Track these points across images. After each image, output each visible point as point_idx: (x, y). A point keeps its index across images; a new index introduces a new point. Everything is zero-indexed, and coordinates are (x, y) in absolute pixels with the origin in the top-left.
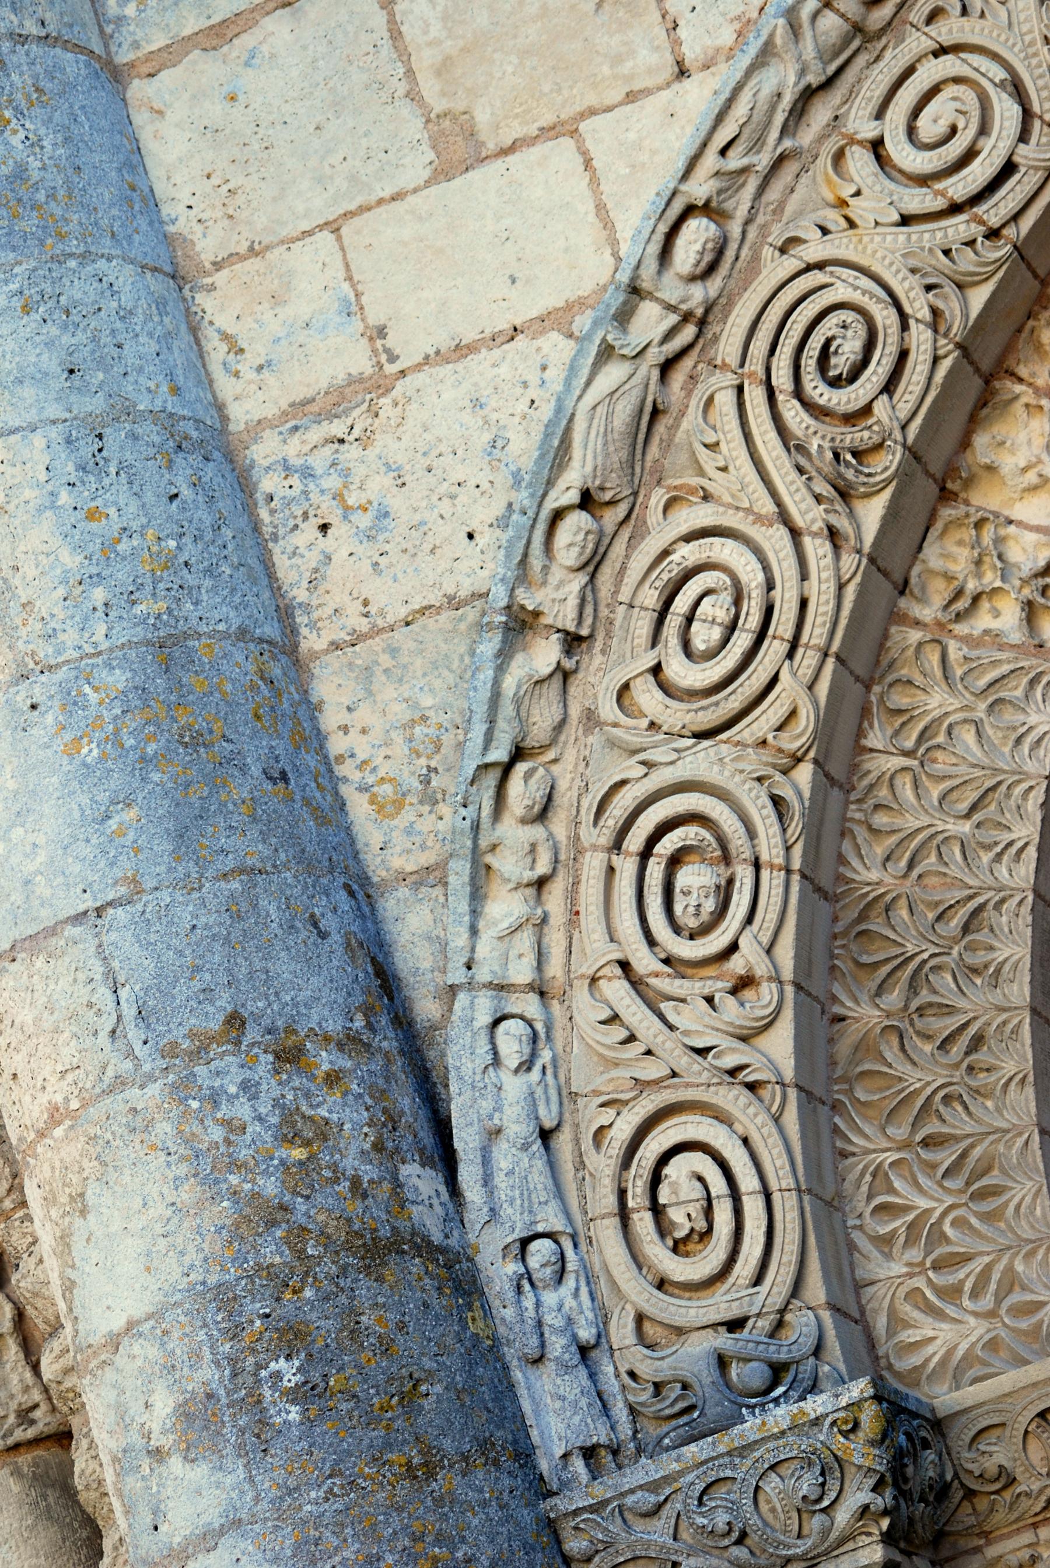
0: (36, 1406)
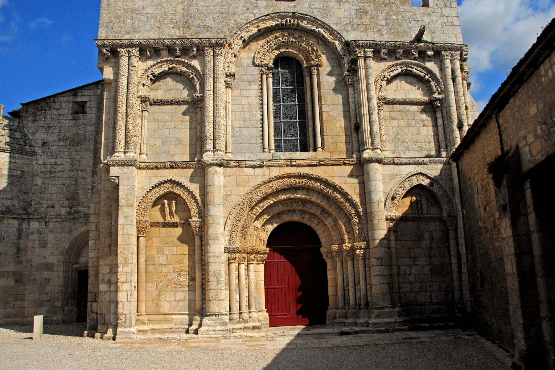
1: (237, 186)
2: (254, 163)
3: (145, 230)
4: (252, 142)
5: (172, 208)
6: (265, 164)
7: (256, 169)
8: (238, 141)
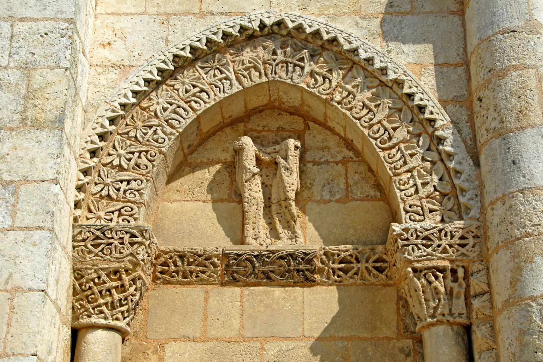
0: (463, 314)
3: (122, 288)
5: (285, 174)
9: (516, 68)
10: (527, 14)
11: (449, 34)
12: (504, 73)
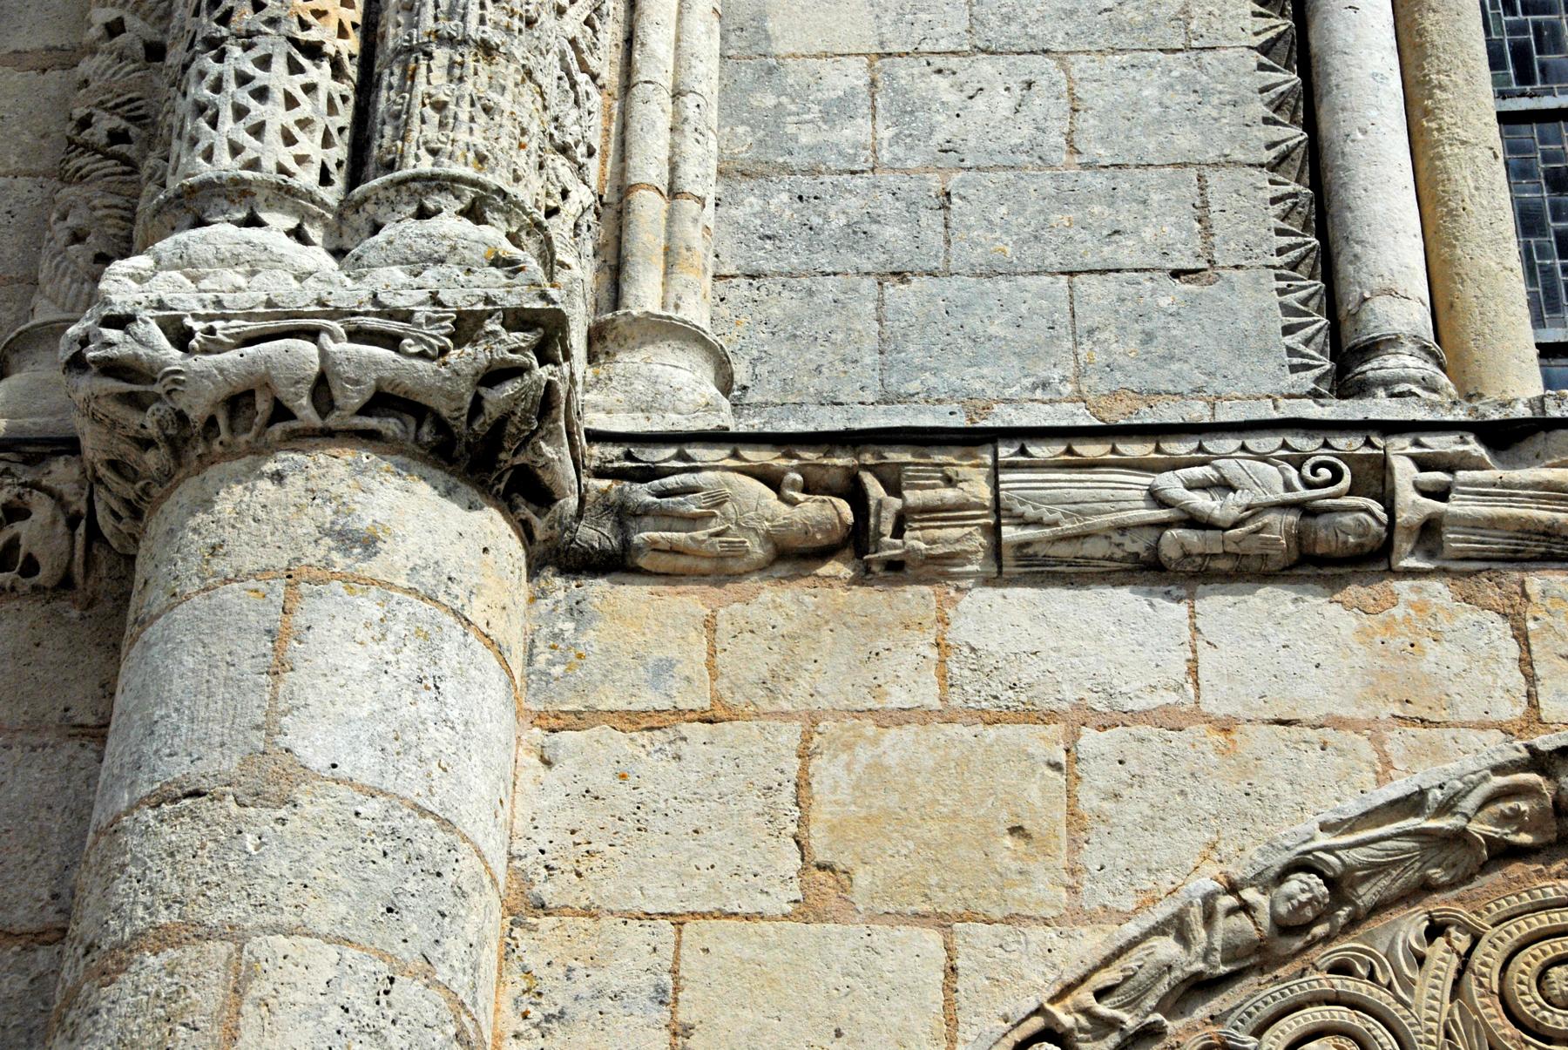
1: (805, 911)
2: (1171, 483)
4: (1126, 253)
6: (1412, 505)
7: (1216, 605)
8: (857, 234)
9: (163, 938)
10: (258, 727)
11: (43, 813)
12: (120, 962)
